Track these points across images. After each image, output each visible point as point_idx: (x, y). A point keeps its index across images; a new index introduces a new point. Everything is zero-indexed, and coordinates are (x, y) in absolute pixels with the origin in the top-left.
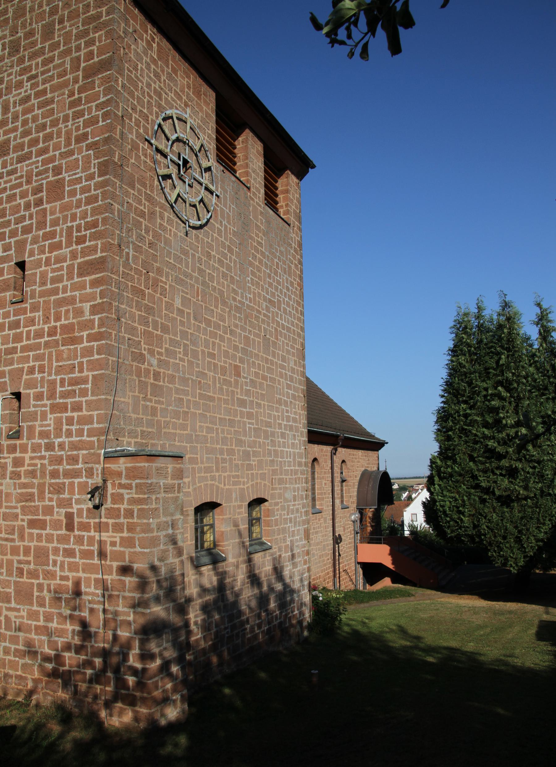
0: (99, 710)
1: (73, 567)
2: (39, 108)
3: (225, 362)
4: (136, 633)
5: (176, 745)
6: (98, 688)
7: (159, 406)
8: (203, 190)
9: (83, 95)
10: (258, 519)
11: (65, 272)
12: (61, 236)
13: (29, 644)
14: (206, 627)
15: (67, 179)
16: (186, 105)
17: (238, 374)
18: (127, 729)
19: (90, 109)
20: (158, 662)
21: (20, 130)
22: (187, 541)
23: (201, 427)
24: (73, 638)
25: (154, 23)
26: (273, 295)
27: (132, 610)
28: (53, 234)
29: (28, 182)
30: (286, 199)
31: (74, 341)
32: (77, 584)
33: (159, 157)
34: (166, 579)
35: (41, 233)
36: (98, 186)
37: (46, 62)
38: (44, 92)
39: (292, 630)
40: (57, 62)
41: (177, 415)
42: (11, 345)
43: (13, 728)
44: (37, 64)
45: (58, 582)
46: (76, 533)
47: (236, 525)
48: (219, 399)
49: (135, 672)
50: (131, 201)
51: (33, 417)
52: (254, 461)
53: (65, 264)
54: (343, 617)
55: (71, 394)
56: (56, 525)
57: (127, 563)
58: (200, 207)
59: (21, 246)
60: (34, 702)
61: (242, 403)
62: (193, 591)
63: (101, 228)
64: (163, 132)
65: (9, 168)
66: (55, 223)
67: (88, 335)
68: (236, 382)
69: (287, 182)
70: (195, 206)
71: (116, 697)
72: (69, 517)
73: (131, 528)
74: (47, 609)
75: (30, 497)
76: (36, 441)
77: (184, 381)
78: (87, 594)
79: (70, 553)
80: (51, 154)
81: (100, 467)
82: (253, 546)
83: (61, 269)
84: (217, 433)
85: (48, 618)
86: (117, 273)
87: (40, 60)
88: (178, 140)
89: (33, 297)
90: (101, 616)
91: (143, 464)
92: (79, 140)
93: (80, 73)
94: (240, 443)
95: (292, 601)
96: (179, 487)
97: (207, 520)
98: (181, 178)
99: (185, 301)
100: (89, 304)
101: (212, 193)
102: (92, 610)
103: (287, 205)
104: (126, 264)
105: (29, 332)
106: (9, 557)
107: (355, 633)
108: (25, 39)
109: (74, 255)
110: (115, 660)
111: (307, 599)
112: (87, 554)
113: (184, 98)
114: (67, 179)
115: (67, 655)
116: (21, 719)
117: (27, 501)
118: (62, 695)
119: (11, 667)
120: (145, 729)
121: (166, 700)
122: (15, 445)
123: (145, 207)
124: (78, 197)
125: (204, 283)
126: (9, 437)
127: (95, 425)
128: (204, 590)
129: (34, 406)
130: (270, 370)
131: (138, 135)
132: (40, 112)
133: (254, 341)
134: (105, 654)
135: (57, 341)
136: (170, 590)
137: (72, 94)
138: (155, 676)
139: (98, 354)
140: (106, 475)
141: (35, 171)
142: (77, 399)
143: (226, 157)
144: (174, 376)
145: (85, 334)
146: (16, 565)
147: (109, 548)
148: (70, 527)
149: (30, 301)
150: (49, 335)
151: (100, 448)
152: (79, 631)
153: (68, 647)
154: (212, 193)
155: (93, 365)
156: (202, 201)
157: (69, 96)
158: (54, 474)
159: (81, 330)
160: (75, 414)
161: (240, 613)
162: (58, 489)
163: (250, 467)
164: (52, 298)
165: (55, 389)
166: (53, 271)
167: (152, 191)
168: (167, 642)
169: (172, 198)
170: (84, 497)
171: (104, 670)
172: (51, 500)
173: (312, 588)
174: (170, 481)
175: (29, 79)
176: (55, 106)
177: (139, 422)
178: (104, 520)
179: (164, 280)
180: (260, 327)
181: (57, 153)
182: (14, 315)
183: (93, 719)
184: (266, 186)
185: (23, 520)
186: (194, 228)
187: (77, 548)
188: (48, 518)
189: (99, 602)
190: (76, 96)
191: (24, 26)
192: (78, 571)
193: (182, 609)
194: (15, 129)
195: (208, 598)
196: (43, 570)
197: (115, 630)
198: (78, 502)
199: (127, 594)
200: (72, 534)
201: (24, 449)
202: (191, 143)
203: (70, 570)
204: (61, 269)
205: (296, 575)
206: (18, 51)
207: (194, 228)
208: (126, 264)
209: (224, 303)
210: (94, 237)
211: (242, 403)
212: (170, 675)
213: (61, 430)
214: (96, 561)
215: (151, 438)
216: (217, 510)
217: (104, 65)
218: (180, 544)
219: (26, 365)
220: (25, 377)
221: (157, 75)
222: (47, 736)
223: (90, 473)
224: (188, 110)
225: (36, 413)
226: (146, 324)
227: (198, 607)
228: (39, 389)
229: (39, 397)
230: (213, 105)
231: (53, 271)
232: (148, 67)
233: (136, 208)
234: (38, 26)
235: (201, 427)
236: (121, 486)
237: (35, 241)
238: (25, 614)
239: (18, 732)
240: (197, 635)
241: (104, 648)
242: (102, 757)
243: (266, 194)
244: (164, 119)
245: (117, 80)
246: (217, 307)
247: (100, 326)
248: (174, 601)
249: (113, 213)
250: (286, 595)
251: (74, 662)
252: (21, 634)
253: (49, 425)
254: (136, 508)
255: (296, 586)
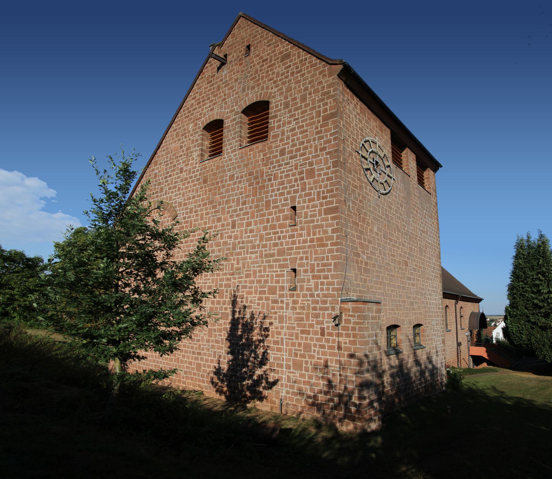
0: (336, 423)
1: (324, 353)
2: (300, 134)
3: (400, 259)
4: (356, 386)
5: (376, 442)
6: (336, 412)
7: (368, 278)
8: (386, 176)
9: (323, 129)
10: (419, 334)
11: (317, 212)
12: (314, 195)
13: (300, 389)
14: (392, 384)
15: (316, 168)
16: (376, 135)
17: (407, 265)
18: (350, 432)
19: (327, 136)
20: (367, 401)
21: (291, 144)
22: (383, 342)
23: (388, 289)
24: (323, 387)
25: (351, 90)
26: (424, 228)
27: (354, 375)
28: (310, 194)
29: (296, 169)
30: (428, 181)
31: (323, 245)
32: (326, 362)
33: (363, 159)
34: (372, 361)
35: (304, 193)
36: (333, 172)
37: (303, 113)
38: (303, 126)
39: (437, 387)
40: (308, 112)
41: (376, 283)
42: (290, 246)
43: (291, 429)
44: (298, 113)
45: (316, 360)
46: (326, 337)
47: (407, 336)
48: (397, 276)
49: (355, 405)
50: (350, 180)
51: (303, 281)
52: (415, 306)
53: (317, 209)
54: (463, 381)
55: (323, 271)
56: (316, 333)
57: (352, 352)
58: (385, 184)
59: (293, 199)
60: (301, 417)
61: (409, 279)
62: (386, 367)
63: (335, 192)
64: (365, 148)
65: (286, 162)
66: (311, 189)
67: (331, 243)
68: (406, 268)
69: (428, 173)
70: (382, 184)
71: (345, 417)
72: (322, 329)
73: (355, 336)
74: (310, 373)
75: (302, 319)
76: (305, 292)
77: (380, 267)
78: (331, 366)
79: (323, 347)
80: (307, 156)
81: (338, 306)
82: (416, 346)
83: (315, 211)
84: (397, 293)
85: (310, 377)
86: (344, 214)
87: (300, 111)
88: (372, 152)
89: (301, 223)
90: (338, 378)
91: (361, 306)
92: (321, 150)
93: (321, 118)
94: (408, 297)
95: (437, 373)
96: (379, 318)
97: (392, 333)
98: (375, 170)
99: (379, 229)
100: (330, 228)
101: (391, 178)
102: (334, 375)
103: (429, 185)
104: (349, 210)
105: (299, 240)
106: (290, 347)
107: (470, 389)
108: (292, 101)
109: (321, 205)
110: (345, 399)
111: (444, 372)
112: (332, 348)
113: (375, 132)
114: (316, 168)
115: (320, 395)
116: (294, 426)
117: (300, 321)
118: (318, 415)
119: (290, 400)
120: (360, 433)
121: (371, 420)
122: (294, 294)
123: (357, 183)
124: (322, 177)
125: (388, 221)
126: (290, 290)
127: (336, 286)
128: (391, 367)
129: (303, 276)
130: (423, 263)
131: (352, 149)
132: (301, 136)
133: (414, 249)
134: (340, 396)
135: (314, 245)
136: (375, 367)
137: (317, 128)
138: (366, 407)
139: (336, 252)
140: (342, 310)
141: (299, 164)
142: (326, 273)
143: (397, 161)
144: (375, 264)
145: (329, 242)
146: (293, 351)
147: (343, 345)
148: (323, 334)
149: (299, 225)
150: (310, 242)
151: (338, 297)
152: (326, 384)
153: (320, 392)
154: (391, 178)
155: (334, 258)
156: (386, 181)
157: (316, 129)
158: (314, 309)
159: (327, 240)
160: (325, 281)
161: (411, 378)
162: (317, 316)
163: (413, 309)
164: (311, 225)
165: (314, 268)
166: (311, 211)
167: (360, 176)
168: (372, 391)
169: (371, 180)
170: (330, 320)
171: (339, 404)
172: (312, 321)
173: (447, 367)
174: (374, 314)
175: (294, 120)
176: (308, 133)
177: (358, 285)
178: (340, 331)
179: (368, 218)
180: (417, 243)
181: (310, 156)
182: (291, 232)
183: (332, 427)
184: (418, 175)
185: (298, 330)
186: (383, 194)
187: (326, 344)
188: (311, 329)
189: (337, 371)
190: (319, 129)
191: (291, 95)
192: (327, 355)
193: (380, 376)
194: (288, 143)
195: (393, 370)
196: (308, 355)
197: (346, 384)
198: (327, 322)
199: (352, 367)
200: (324, 338)
201: (298, 296)
202: (379, 153)
203: (322, 355)
204: (315, 211)
205: (439, 361)
206: (288, 107)
207: (383, 194)
208: (349, 210)
209: (399, 231)
210: (331, 196)
211: (409, 279)
212: (373, 407)
213: (318, 288)
214: (336, 351)
215: (364, 293)
216: (398, 329)
217: (333, 115)
218: (379, 344)
219: (299, 256)
220: (298, 261)
221: (360, 120)
222: (308, 434)
223: (333, 309)
224: (377, 138)
225: (304, 279)
226: (360, 239)
227: (388, 375)
228: (306, 268)
229: (306, 271)
230: (389, 136)
231: (311, 211)
232: (356, 117)
233: (353, 184)
234: (298, 96)
235: (388, 289)
236: (349, 316)
237: (300, 197)
238: (298, 375)
239: (293, 431)
240: (388, 388)
241: (339, 393)
242: (337, 446)
243: (418, 179)
244: (365, 142)
245: (340, 122)
246: (395, 233)
247: (337, 238)
248: (377, 371)
249: (341, 186)
250: (434, 371)
251: (324, 399)
252: (296, 385)
253: (311, 285)
254: (357, 327)
255: (439, 366)
